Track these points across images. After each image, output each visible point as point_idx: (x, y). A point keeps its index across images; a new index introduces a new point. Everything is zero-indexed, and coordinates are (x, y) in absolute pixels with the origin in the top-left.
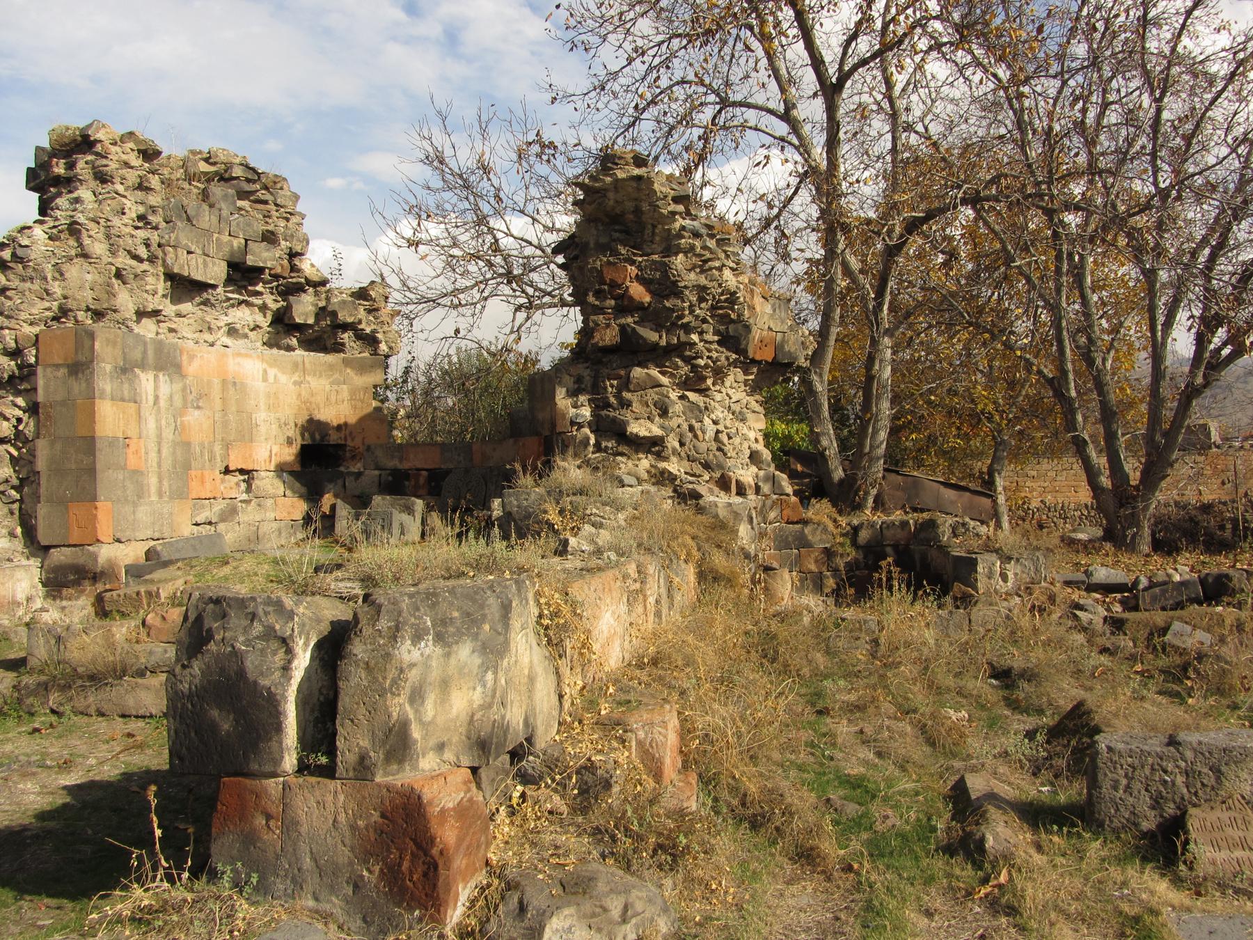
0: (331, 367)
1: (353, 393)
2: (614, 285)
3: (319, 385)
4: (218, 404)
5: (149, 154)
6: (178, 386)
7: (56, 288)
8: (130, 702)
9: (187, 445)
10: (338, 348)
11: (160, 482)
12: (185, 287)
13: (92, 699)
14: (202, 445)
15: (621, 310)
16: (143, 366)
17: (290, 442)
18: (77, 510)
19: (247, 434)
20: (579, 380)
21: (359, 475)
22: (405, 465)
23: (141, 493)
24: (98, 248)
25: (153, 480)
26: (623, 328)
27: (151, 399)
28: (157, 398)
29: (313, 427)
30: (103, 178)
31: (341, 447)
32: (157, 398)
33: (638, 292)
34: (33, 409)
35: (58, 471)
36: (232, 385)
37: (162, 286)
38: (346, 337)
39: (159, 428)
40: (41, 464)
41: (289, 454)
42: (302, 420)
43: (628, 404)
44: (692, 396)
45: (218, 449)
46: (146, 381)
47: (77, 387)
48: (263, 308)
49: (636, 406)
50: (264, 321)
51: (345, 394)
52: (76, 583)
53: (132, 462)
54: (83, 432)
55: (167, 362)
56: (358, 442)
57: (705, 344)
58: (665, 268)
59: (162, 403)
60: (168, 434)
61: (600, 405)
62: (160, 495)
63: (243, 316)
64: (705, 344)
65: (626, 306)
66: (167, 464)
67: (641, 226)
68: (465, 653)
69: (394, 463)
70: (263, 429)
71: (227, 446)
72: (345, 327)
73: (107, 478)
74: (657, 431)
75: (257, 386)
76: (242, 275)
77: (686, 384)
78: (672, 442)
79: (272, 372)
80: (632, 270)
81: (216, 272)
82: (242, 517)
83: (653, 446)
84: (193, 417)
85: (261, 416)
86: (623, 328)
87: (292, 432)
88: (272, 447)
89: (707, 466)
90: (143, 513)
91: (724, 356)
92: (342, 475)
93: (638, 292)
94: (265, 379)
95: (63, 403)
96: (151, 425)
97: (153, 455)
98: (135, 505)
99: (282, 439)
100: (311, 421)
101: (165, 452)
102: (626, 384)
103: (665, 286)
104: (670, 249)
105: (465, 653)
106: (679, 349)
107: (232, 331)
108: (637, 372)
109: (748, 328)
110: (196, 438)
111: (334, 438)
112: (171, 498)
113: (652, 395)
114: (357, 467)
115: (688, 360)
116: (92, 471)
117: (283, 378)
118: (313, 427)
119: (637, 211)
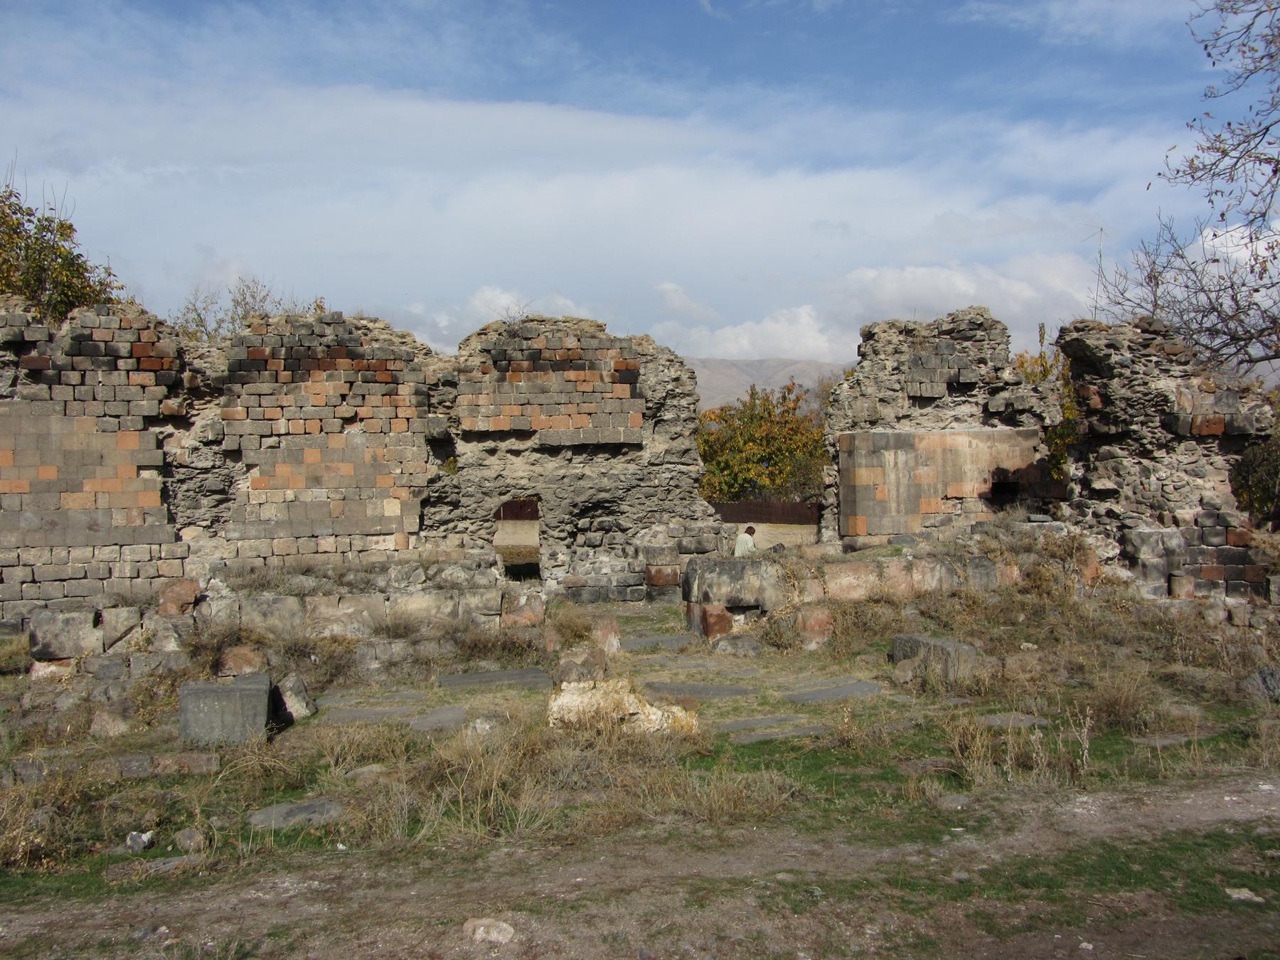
0: (1009, 437)
1: (1022, 451)
3: (1003, 447)
4: (940, 462)
5: (908, 332)
6: (912, 455)
7: (850, 413)
9: (919, 485)
11: (898, 505)
12: (921, 401)
14: (929, 486)
16: (886, 448)
17: (985, 481)
19: (959, 477)
23: (885, 511)
24: (870, 390)
25: (893, 505)
27: (892, 464)
28: (896, 464)
29: (999, 473)
32: (896, 464)
36: (950, 453)
37: (907, 403)
38: (1024, 418)
39: (898, 479)
41: (986, 488)
42: (992, 469)
44: (1145, 462)
45: (940, 486)
46: (889, 456)
47: (851, 462)
48: (977, 404)
49: (1101, 471)
50: (977, 411)
51: (1018, 453)
53: (879, 496)
55: (904, 443)
57: (1150, 432)
59: (900, 465)
60: (904, 481)
62: (898, 511)
63: (965, 410)
64: (1150, 432)
66: (903, 495)
68: (725, 578)
70: (969, 474)
71: (946, 485)
72: (1022, 412)
73: (862, 504)
74: (1110, 485)
76: (959, 388)
79: (974, 442)
80: (1093, 388)
81: (941, 389)
82: (954, 523)
84: (922, 471)
85: (968, 467)
88: (973, 485)
89: (1152, 507)
90: (886, 521)
91: (1162, 435)
94: (970, 446)
96: (892, 477)
97: (894, 493)
98: (881, 517)
99: (981, 479)
100: (998, 469)
101: (901, 490)
104: (1112, 377)
105: (725, 578)
107: (957, 419)
109: (1177, 418)
110: (925, 482)
111: (1011, 478)
112: (906, 513)
113: (1111, 463)
116: (854, 501)
117: (981, 445)
118: (999, 473)
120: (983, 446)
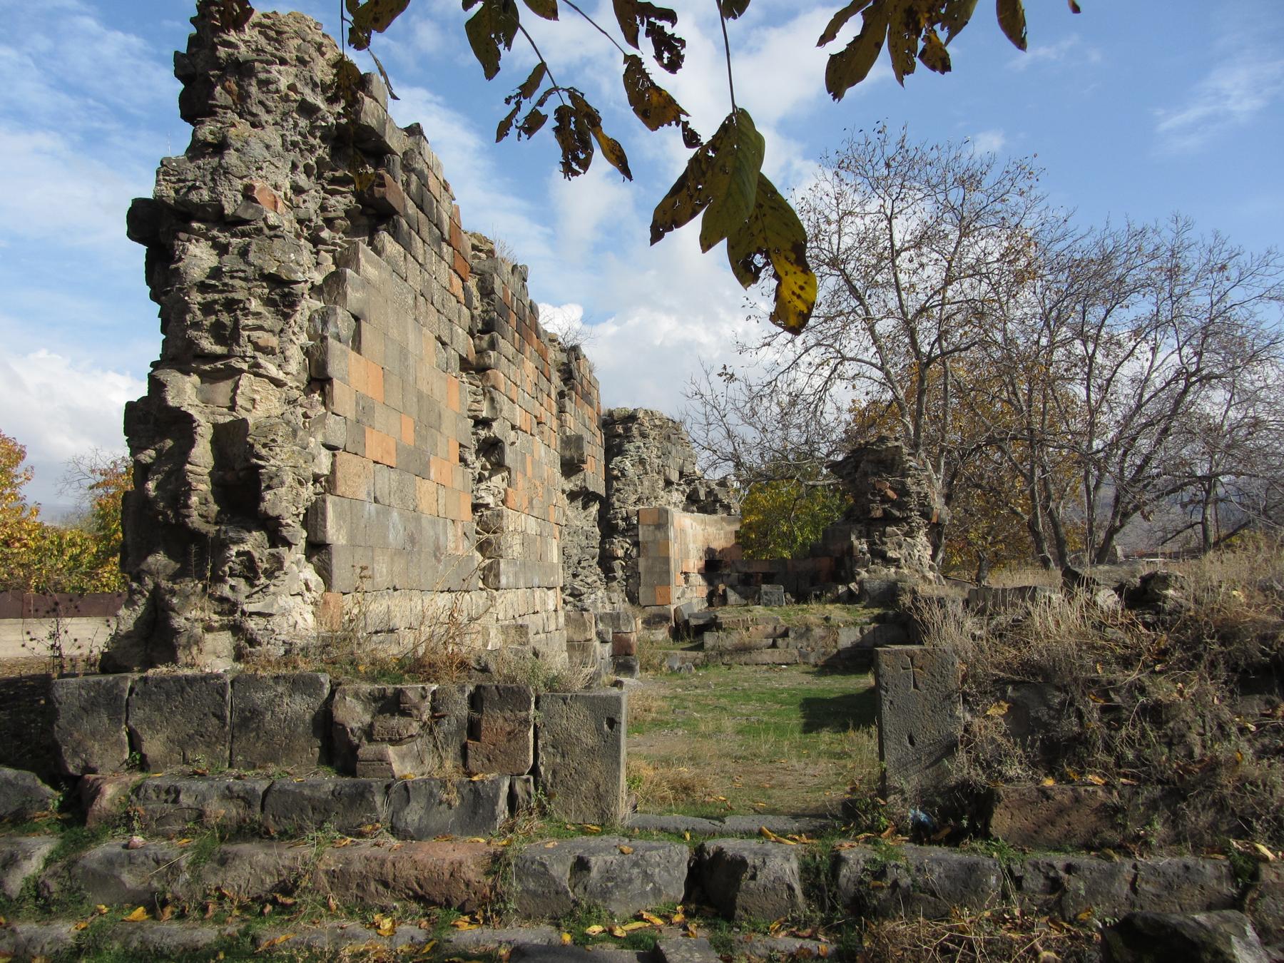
0: (716, 521)
1: (726, 534)
2: (880, 490)
3: (711, 530)
8: (759, 659)
10: (714, 512)
13: (744, 658)
15: (882, 502)
18: (659, 590)
20: (860, 532)
21: (729, 575)
22: (751, 571)
26: (884, 510)
29: (709, 552)
30: (644, 436)
31: (720, 561)
33: (891, 493)
34: (636, 544)
35: (649, 570)
40: (641, 569)
41: (701, 564)
43: (885, 543)
47: (659, 535)
48: (683, 492)
52: (660, 622)
54: (662, 555)
56: (728, 559)
58: (904, 484)
61: (871, 544)
65: (886, 499)
67: (893, 464)
69: (745, 569)
75: (690, 531)
77: (906, 535)
78: (903, 561)
83: (895, 562)
85: (691, 546)
86: (884, 510)
87: (702, 554)
92: (722, 576)
93: (891, 493)
95: (653, 542)
102: (884, 534)
103: (903, 491)
104: (904, 474)
106: (906, 519)
108: (888, 529)
111: (718, 557)
113: (895, 539)
114: (727, 571)
115: (908, 524)
116: (668, 572)
118: (709, 552)
119: (893, 459)
120: (699, 528)
